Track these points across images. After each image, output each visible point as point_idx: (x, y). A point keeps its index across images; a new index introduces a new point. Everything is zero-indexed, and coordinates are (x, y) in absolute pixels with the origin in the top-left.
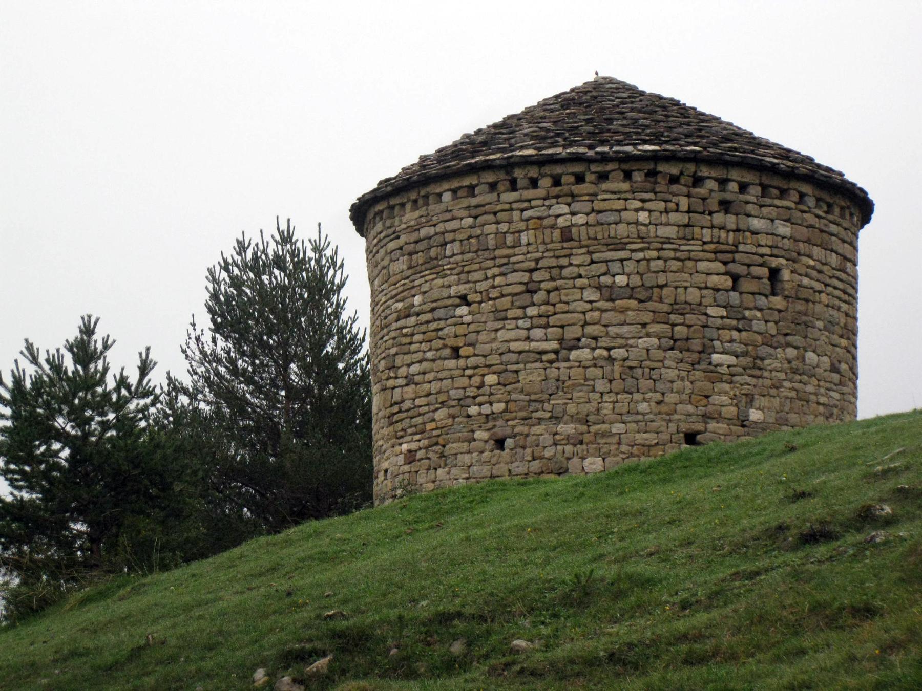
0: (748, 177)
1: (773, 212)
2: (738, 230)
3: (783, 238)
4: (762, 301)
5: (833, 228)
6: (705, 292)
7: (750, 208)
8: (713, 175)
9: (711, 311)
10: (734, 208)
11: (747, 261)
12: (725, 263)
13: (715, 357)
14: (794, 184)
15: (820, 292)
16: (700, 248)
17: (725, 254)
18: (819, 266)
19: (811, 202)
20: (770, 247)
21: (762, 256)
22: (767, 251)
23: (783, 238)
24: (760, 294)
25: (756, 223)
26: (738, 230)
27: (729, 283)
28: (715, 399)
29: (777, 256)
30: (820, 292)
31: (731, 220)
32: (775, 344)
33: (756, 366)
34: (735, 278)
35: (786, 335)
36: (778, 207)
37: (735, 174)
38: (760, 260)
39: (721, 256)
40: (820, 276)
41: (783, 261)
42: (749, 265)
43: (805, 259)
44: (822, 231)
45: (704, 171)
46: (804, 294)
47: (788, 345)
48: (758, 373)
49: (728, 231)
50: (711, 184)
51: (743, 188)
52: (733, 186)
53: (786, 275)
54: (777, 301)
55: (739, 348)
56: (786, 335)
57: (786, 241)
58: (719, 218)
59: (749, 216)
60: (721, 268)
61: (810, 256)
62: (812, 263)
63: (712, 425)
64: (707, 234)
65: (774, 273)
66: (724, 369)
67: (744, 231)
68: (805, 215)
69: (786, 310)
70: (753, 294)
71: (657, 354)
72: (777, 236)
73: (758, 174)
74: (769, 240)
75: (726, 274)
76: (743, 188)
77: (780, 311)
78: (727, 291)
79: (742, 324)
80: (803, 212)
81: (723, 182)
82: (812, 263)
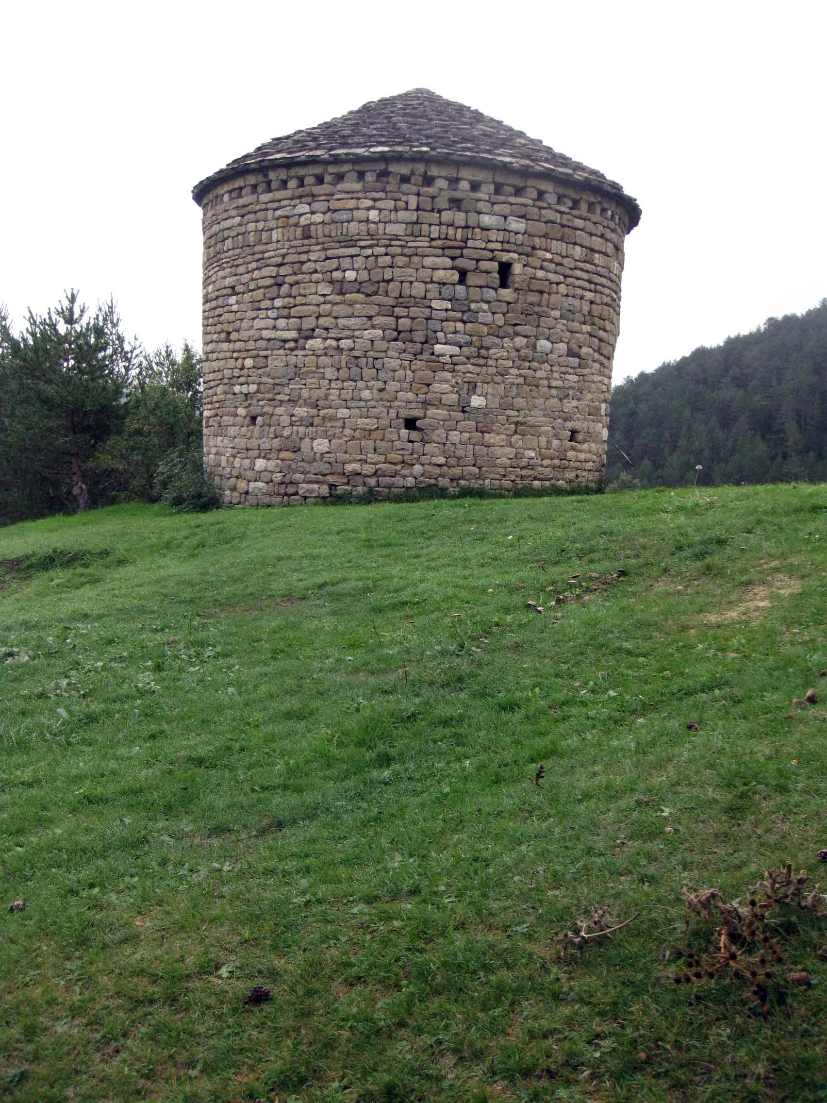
0: (480, 176)
1: (507, 209)
2: (467, 227)
3: (516, 233)
4: (490, 294)
5: (579, 223)
6: (430, 286)
7: (481, 205)
8: (443, 174)
9: (435, 304)
10: (464, 205)
11: (475, 256)
12: (453, 259)
13: (438, 348)
14: (531, 182)
15: (558, 284)
16: (427, 244)
17: (453, 249)
18: (558, 259)
19: (551, 198)
20: (502, 242)
21: (492, 251)
22: (498, 246)
23: (516, 233)
24: (488, 287)
25: (486, 220)
26: (467, 227)
27: (456, 277)
28: (436, 387)
29: (508, 251)
30: (558, 284)
31: (460, 218)
32: (501, 334)
33: (481, 354)
34: (463, 274)
35: (516, 325)
36: (511, 204)
37: (465, 173)
38: (490, 255)
39: (447, 252)
40: (559, 268)
41: (515, 256)
42: (478, 261)
43: (541, 253)
44: (563, 226)
45: (434, 171)
46: (537, 285)
47: (517, 334)
48: (482, 361)
49: (457, 228)
50: (441, 183)
51: (475, 187)
52: (464, 185)
53: (517, 269)
54: (507, 294)
55: (461, 338)
56: (516, 325)
57: (520, 236)
58: (447, 216)
59: (479, 213)
60: (448, 262)
61: (546, 250)
62: (549, 256)
63: (432, 411)
64: (435, 232)
65: (505, 269)
66: (447, 359)
67: (473, 228)
68: (543, 211)
69: (517, 301)
70: (481, 287)
71: (381, 345)
72: (509, 232)
73: (491, 173)
74: (501, 236)
75: (453, 268)
76: (475, 187)
77: (508, 303)
78: (453, 285)
79: (466, 314)
80: (540, 208)
81: (454, 181)
82: (549, 256)
